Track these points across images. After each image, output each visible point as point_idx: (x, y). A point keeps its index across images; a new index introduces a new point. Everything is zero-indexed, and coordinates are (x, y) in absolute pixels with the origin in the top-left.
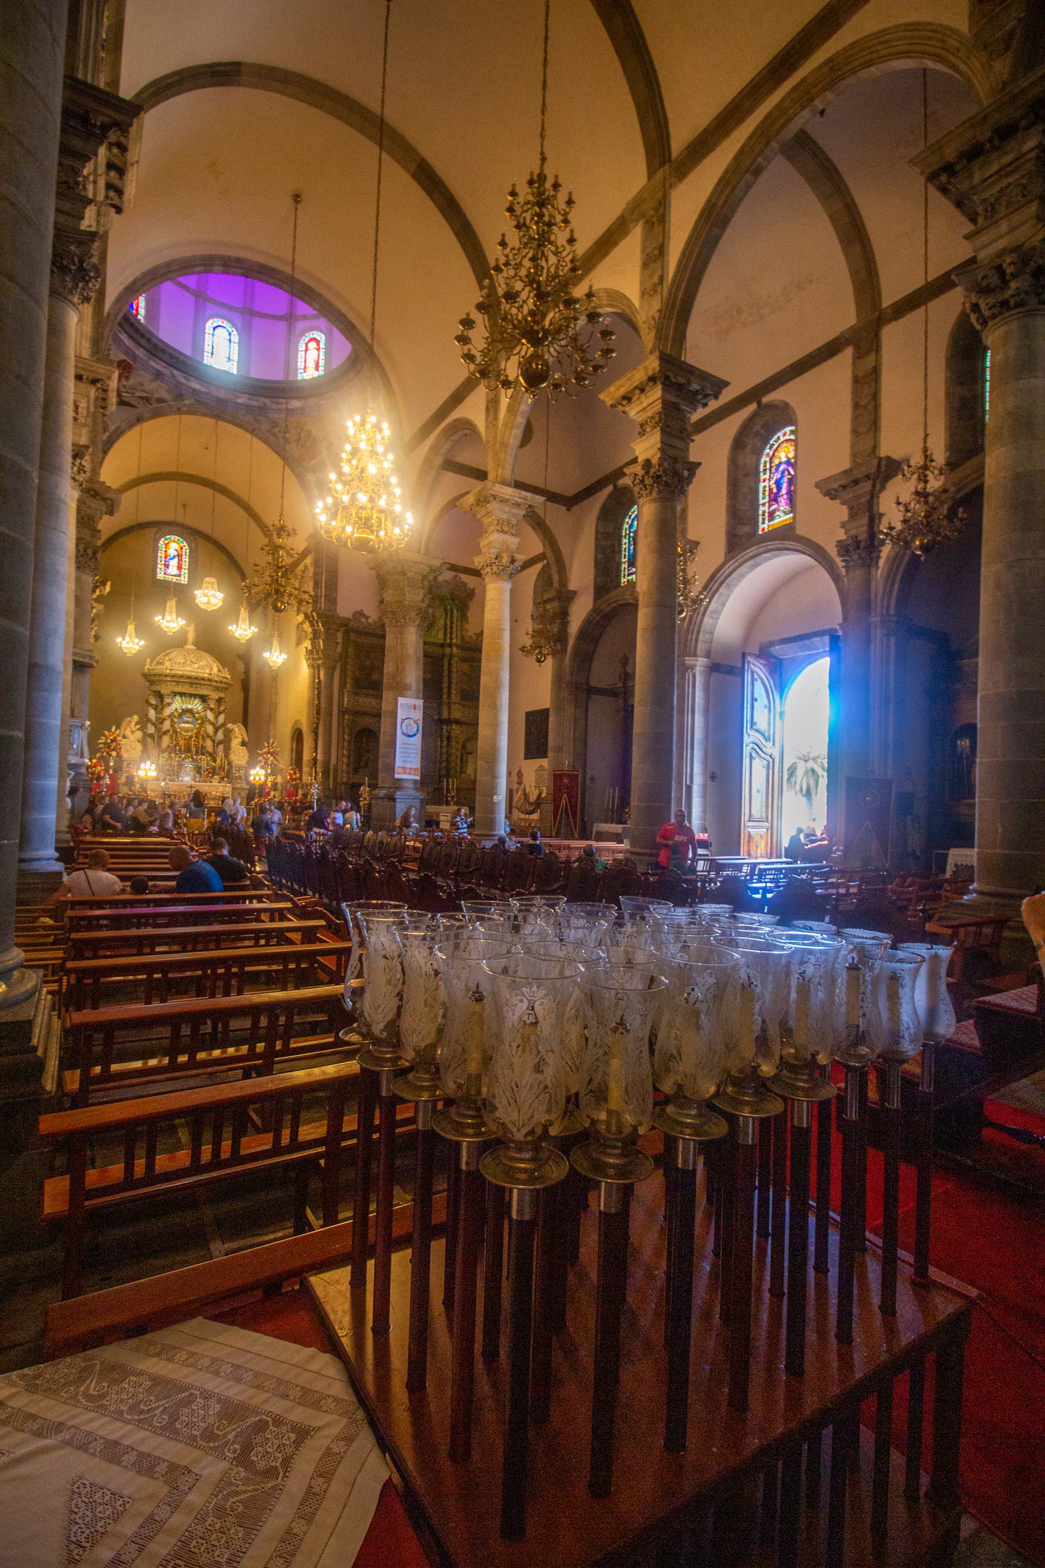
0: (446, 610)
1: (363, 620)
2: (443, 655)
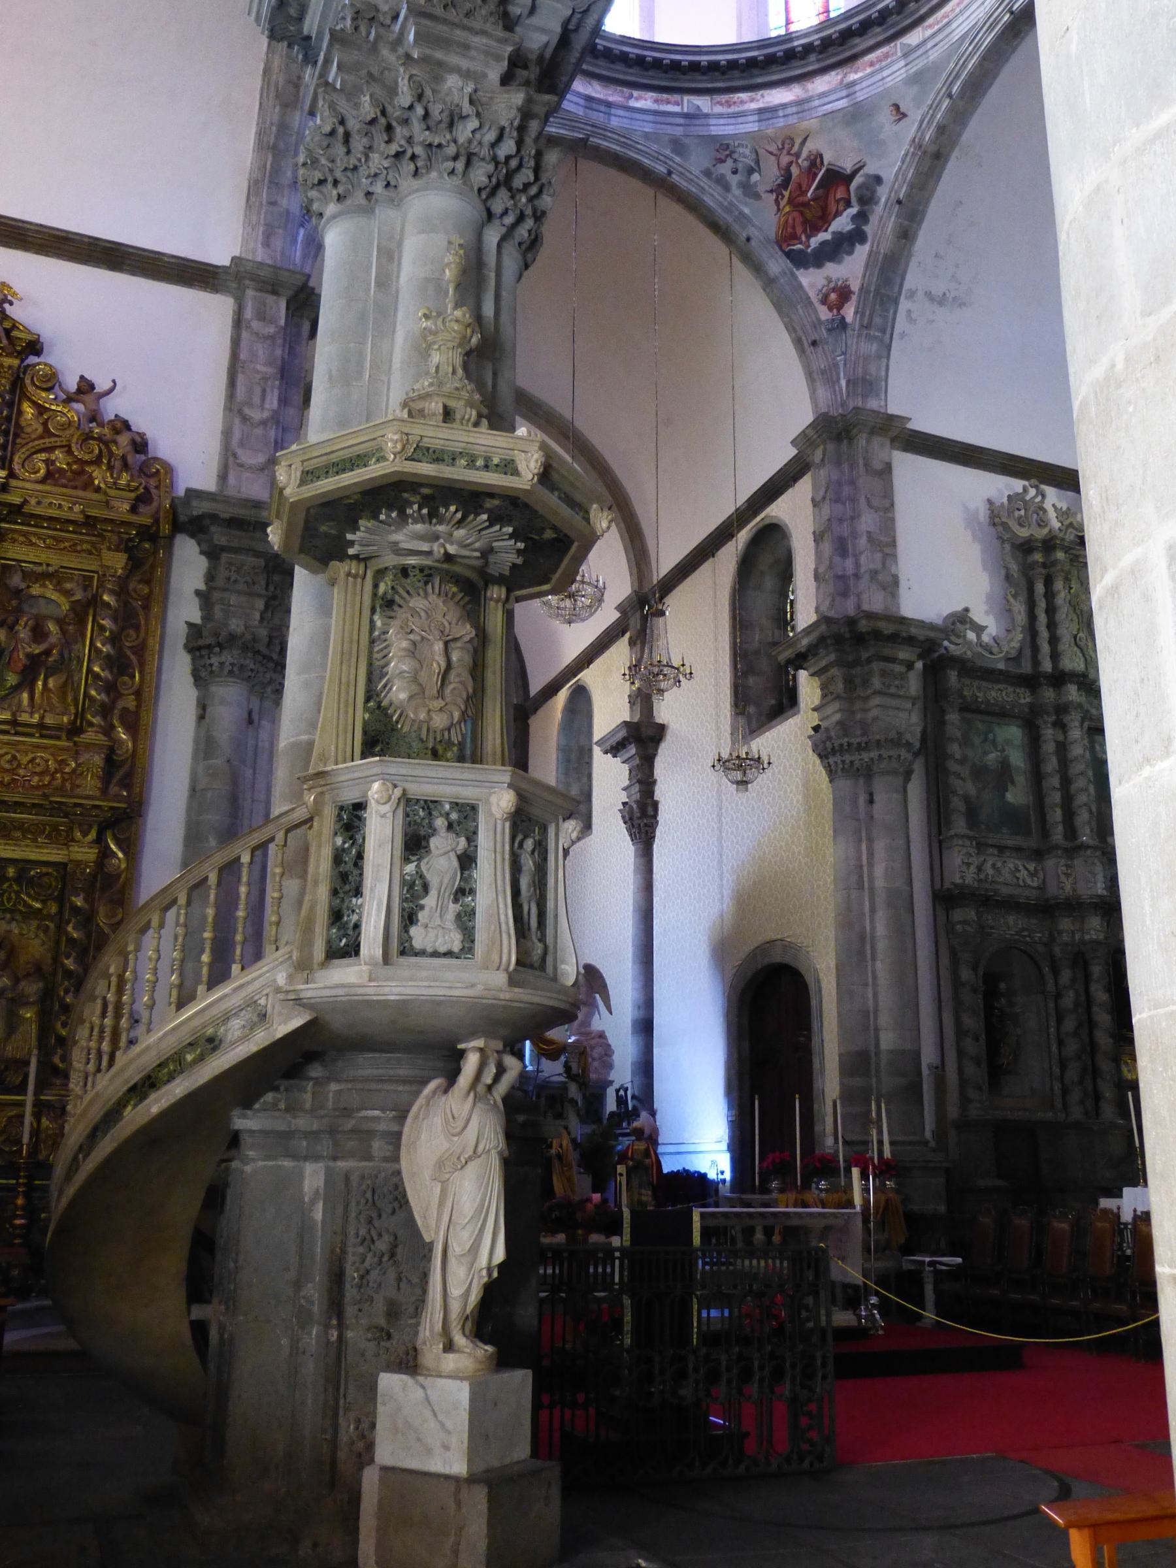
1: (971, 636)
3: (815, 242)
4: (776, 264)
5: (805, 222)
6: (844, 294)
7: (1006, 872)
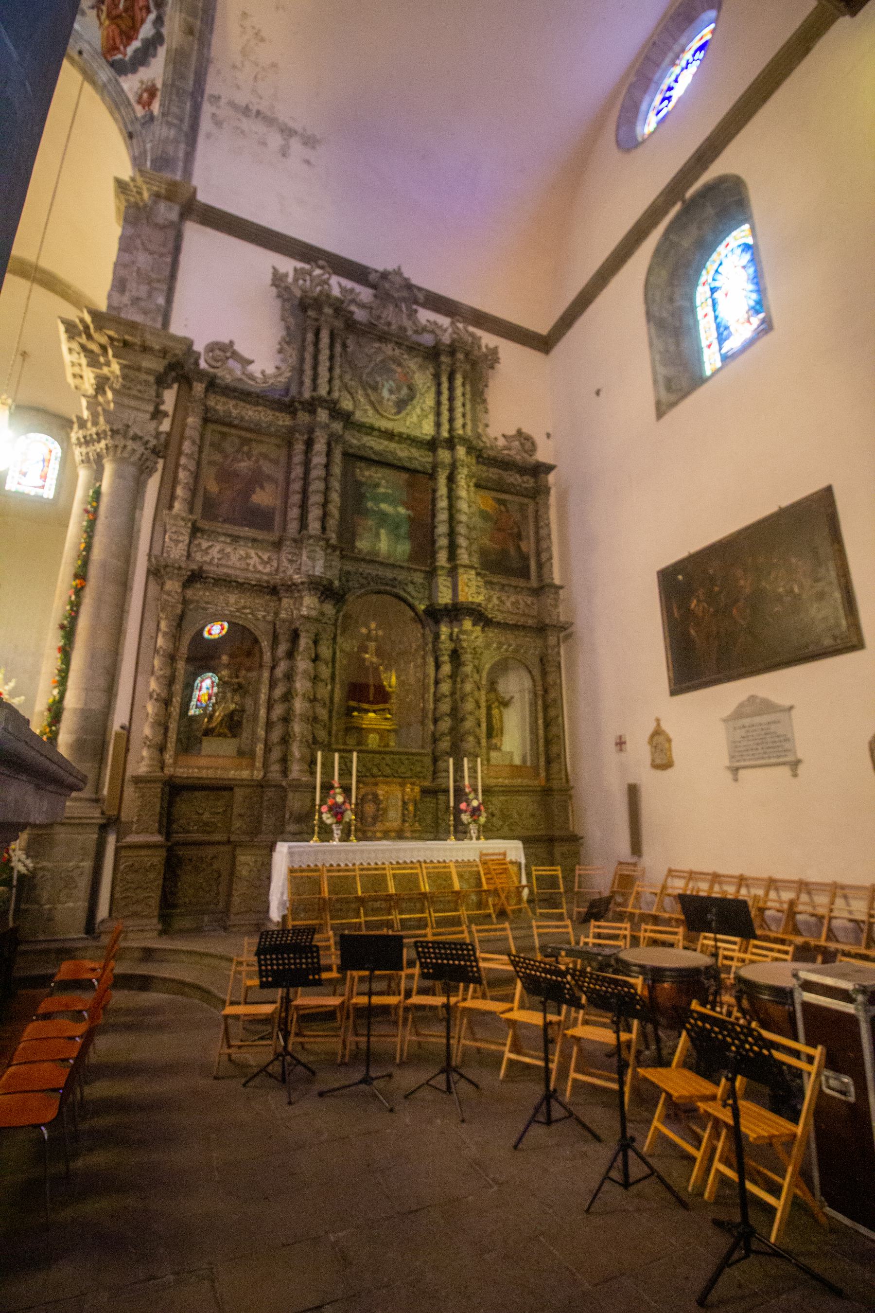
0: (437, 377)
2: (435, 467)
3: (130, 50)
4: (105, 74)
5: (122, 32)
6: (152, 92)
7: (234, 558)
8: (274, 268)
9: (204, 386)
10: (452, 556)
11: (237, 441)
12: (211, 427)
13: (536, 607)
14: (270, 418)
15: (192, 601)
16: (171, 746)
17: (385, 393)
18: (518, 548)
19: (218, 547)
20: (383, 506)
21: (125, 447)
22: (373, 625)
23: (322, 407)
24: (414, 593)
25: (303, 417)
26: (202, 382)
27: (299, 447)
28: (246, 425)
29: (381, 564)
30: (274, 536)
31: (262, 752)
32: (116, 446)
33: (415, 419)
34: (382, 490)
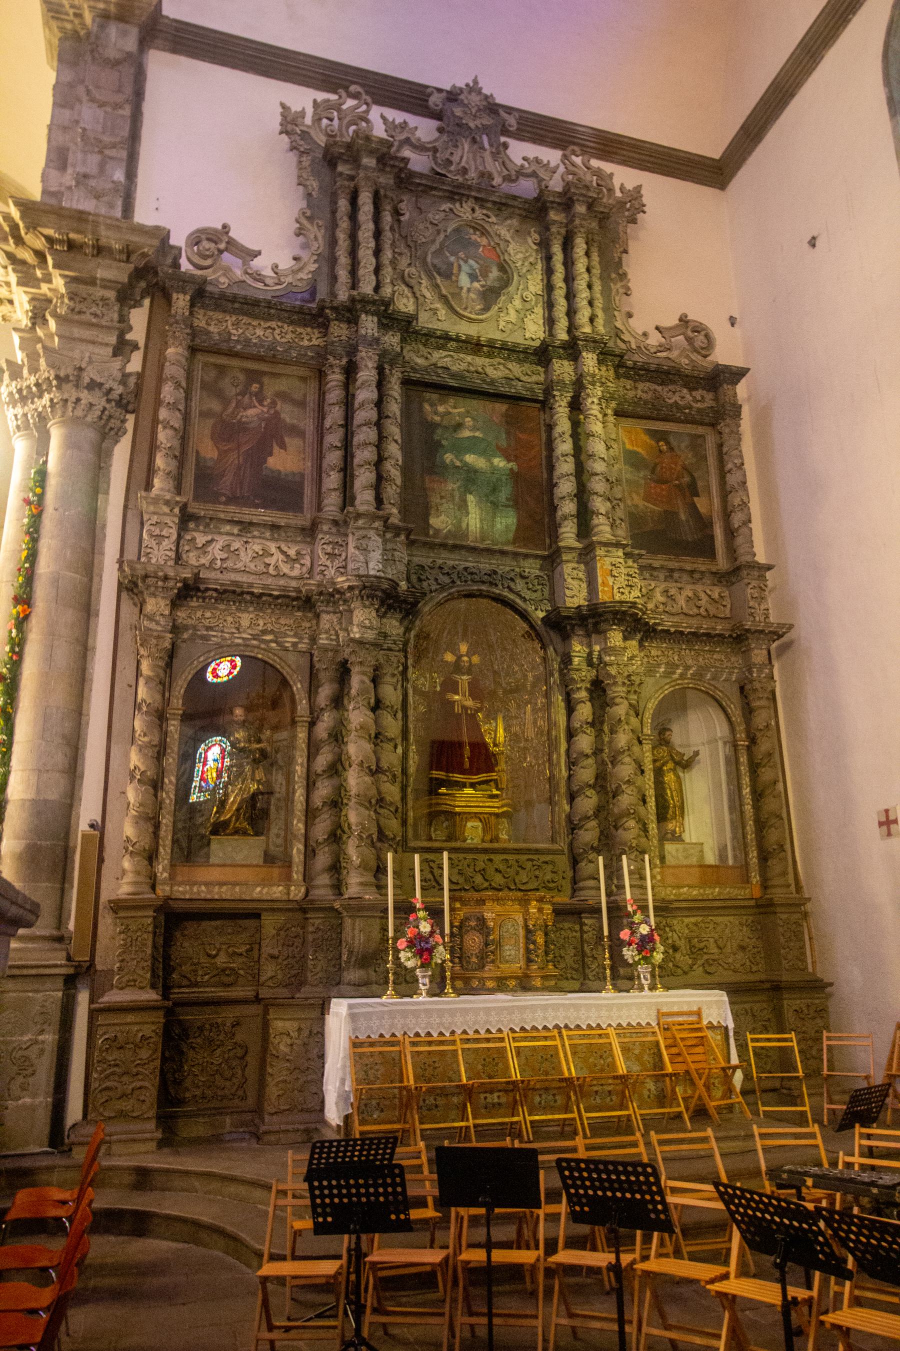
0: (544, 245)
2: (548, 391)
7: (245, 557)
8: (283, 105)
9: (188, 298)
10: (584, 529)
11: (242, 377)
12: (200, 358)
13: (727, 602)
14: (289, 336)
15: (186, 628)
16: (165, 851)
17: (464, 280)
18: (693, 508)
19: (221, 541)
20: (470, 458)
21: (78, 400)
22: (464, 648)
23: (366, 313)
24: (528, 594)
25: (339, 331)
26: (185, 294)
27: (335, 378)
28: (254, 351)
29: (473, 550)
30: (303, 519)
31: (302, 857)
32: (66, 401)
33: (513, 316)
34: (466, 433)
